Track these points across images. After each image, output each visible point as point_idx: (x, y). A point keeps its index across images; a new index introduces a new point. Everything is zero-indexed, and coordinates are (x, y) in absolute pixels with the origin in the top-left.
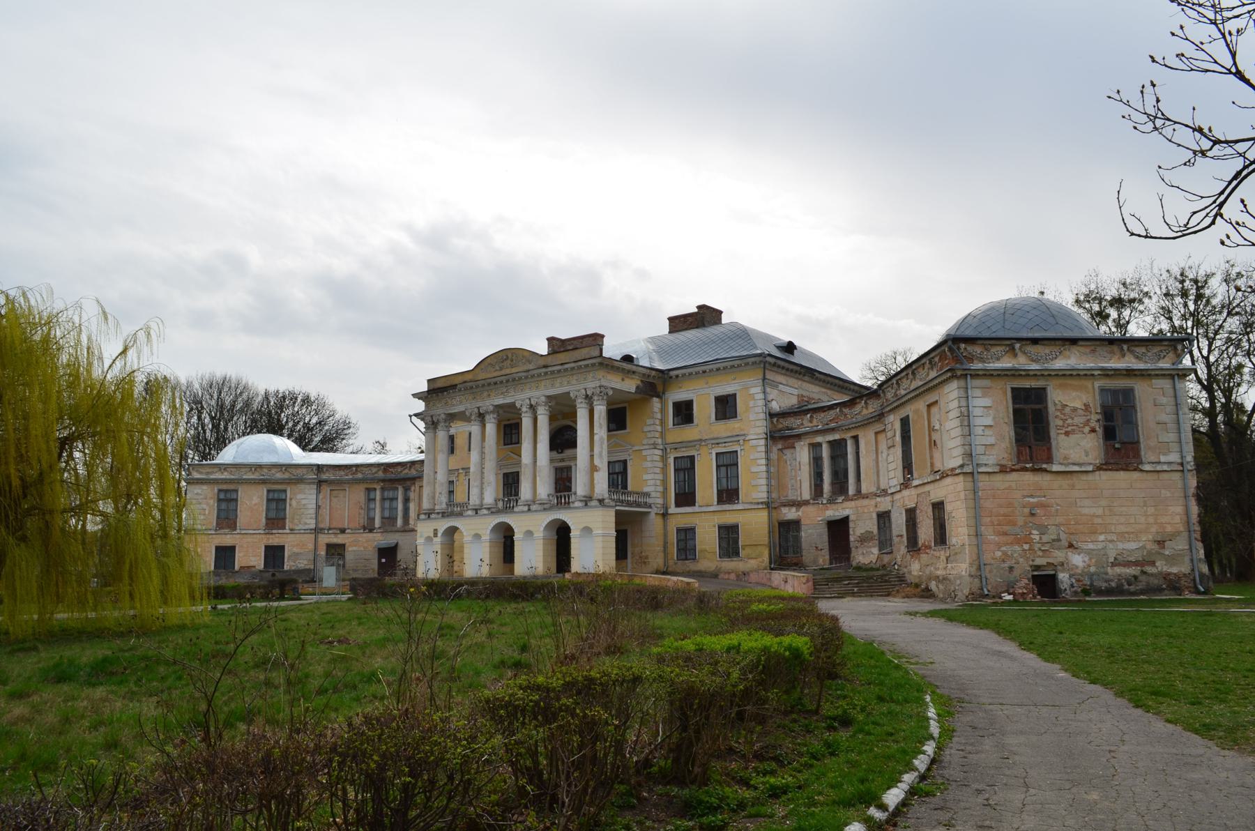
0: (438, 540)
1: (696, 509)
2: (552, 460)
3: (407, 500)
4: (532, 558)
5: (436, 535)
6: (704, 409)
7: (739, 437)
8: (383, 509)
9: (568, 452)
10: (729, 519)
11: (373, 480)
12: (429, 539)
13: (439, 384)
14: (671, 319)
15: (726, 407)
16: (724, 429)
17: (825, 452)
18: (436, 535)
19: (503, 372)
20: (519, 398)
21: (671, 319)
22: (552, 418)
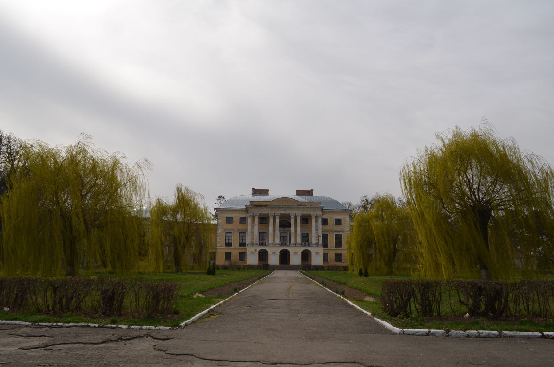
0: (257, 253)
1: (329, 248)
2: (280, 231)
6: (331, 221)
7: (342, 231)
9: (287, 229)
10: (339, 252)
12: (252, 253)
13: (255, 204)
14: (297, 191)
15: (338, 222)
16: (338, 228)
19: (284, 204)
20: (292, 213)
21: (297, 191)
22: (280, 218)
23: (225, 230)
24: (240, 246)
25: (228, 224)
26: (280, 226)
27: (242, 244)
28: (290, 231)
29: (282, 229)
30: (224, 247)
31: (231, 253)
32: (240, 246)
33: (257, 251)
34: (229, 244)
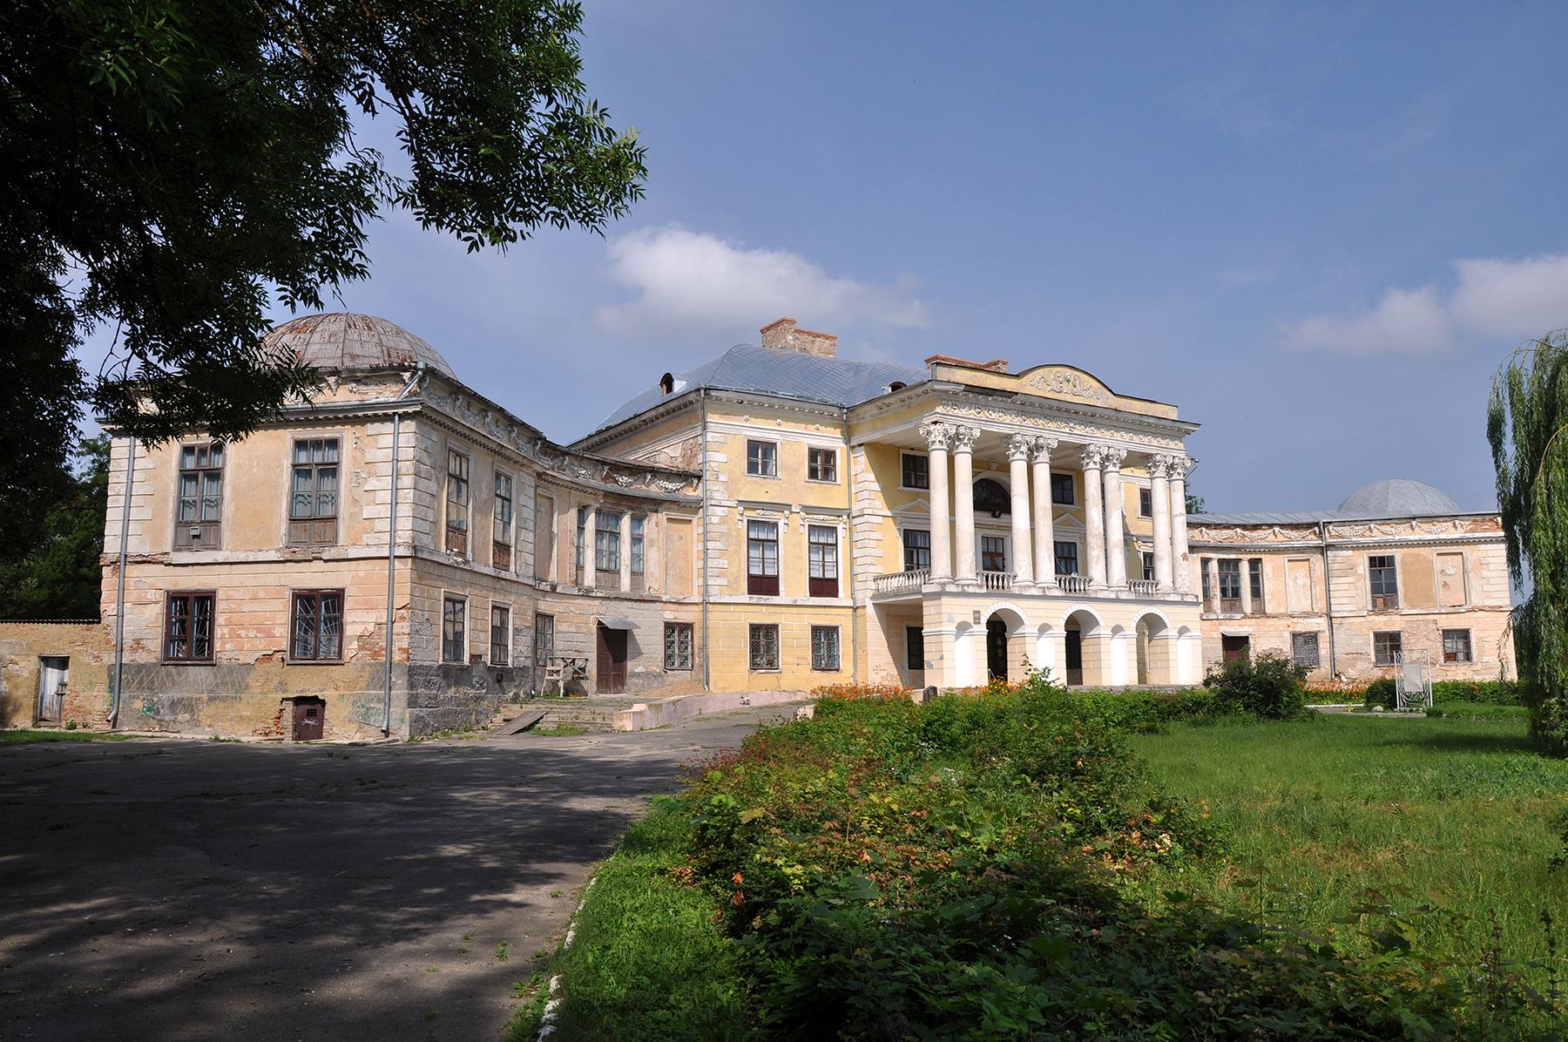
2: (977, 526)
3: (637, 540)
4: (959, 666)
5: (977, 621)
8: (598, 552)
9: (1004, 518)
11: (594, 492)
12: (963, 628)
17: (1214, 567)
18: (977, 621)
22: (977, 464)
23: (748, 505)
24: (813, 593)
25: (754, 478)
26: (978, 505)
27: (823, 587)
28: (1009, 528)
29: (986, 518)
30: (746, 598)
31: (775, 627)
32: (813, 593)
33: (984, 620)
34: (764, 585)
